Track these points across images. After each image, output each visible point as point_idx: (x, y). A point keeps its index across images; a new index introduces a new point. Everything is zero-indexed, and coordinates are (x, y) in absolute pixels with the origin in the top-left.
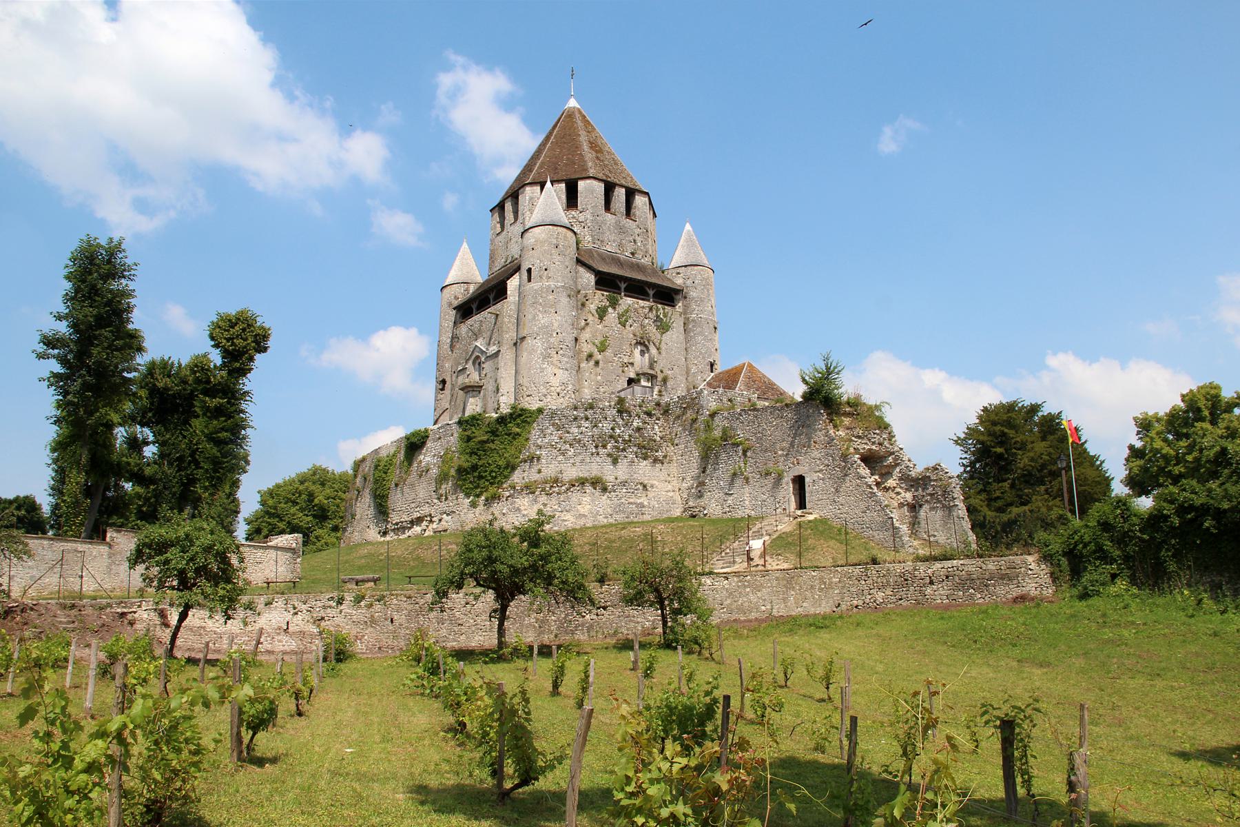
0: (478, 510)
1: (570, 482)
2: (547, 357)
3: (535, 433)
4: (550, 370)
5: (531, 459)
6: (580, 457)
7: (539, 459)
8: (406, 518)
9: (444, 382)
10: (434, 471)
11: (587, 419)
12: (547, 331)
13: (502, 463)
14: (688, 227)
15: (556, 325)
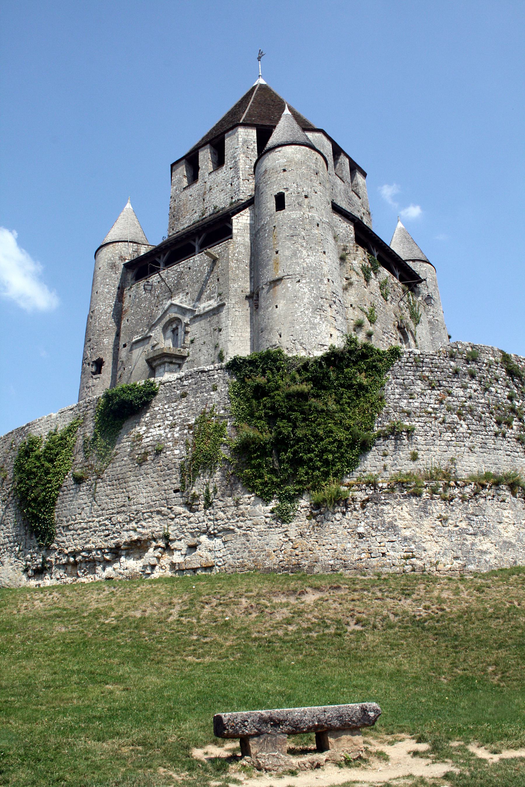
1: (472, 478)
3: (392, 390)
5: (395, 433)
6: (479, 439)
7: (410, 432)
8: (97, 541)
9: (99, 364)
10: (177, 453)
11: (473, 376)
12: (314, 273)
13: (341, 435)
15: (326, 269)
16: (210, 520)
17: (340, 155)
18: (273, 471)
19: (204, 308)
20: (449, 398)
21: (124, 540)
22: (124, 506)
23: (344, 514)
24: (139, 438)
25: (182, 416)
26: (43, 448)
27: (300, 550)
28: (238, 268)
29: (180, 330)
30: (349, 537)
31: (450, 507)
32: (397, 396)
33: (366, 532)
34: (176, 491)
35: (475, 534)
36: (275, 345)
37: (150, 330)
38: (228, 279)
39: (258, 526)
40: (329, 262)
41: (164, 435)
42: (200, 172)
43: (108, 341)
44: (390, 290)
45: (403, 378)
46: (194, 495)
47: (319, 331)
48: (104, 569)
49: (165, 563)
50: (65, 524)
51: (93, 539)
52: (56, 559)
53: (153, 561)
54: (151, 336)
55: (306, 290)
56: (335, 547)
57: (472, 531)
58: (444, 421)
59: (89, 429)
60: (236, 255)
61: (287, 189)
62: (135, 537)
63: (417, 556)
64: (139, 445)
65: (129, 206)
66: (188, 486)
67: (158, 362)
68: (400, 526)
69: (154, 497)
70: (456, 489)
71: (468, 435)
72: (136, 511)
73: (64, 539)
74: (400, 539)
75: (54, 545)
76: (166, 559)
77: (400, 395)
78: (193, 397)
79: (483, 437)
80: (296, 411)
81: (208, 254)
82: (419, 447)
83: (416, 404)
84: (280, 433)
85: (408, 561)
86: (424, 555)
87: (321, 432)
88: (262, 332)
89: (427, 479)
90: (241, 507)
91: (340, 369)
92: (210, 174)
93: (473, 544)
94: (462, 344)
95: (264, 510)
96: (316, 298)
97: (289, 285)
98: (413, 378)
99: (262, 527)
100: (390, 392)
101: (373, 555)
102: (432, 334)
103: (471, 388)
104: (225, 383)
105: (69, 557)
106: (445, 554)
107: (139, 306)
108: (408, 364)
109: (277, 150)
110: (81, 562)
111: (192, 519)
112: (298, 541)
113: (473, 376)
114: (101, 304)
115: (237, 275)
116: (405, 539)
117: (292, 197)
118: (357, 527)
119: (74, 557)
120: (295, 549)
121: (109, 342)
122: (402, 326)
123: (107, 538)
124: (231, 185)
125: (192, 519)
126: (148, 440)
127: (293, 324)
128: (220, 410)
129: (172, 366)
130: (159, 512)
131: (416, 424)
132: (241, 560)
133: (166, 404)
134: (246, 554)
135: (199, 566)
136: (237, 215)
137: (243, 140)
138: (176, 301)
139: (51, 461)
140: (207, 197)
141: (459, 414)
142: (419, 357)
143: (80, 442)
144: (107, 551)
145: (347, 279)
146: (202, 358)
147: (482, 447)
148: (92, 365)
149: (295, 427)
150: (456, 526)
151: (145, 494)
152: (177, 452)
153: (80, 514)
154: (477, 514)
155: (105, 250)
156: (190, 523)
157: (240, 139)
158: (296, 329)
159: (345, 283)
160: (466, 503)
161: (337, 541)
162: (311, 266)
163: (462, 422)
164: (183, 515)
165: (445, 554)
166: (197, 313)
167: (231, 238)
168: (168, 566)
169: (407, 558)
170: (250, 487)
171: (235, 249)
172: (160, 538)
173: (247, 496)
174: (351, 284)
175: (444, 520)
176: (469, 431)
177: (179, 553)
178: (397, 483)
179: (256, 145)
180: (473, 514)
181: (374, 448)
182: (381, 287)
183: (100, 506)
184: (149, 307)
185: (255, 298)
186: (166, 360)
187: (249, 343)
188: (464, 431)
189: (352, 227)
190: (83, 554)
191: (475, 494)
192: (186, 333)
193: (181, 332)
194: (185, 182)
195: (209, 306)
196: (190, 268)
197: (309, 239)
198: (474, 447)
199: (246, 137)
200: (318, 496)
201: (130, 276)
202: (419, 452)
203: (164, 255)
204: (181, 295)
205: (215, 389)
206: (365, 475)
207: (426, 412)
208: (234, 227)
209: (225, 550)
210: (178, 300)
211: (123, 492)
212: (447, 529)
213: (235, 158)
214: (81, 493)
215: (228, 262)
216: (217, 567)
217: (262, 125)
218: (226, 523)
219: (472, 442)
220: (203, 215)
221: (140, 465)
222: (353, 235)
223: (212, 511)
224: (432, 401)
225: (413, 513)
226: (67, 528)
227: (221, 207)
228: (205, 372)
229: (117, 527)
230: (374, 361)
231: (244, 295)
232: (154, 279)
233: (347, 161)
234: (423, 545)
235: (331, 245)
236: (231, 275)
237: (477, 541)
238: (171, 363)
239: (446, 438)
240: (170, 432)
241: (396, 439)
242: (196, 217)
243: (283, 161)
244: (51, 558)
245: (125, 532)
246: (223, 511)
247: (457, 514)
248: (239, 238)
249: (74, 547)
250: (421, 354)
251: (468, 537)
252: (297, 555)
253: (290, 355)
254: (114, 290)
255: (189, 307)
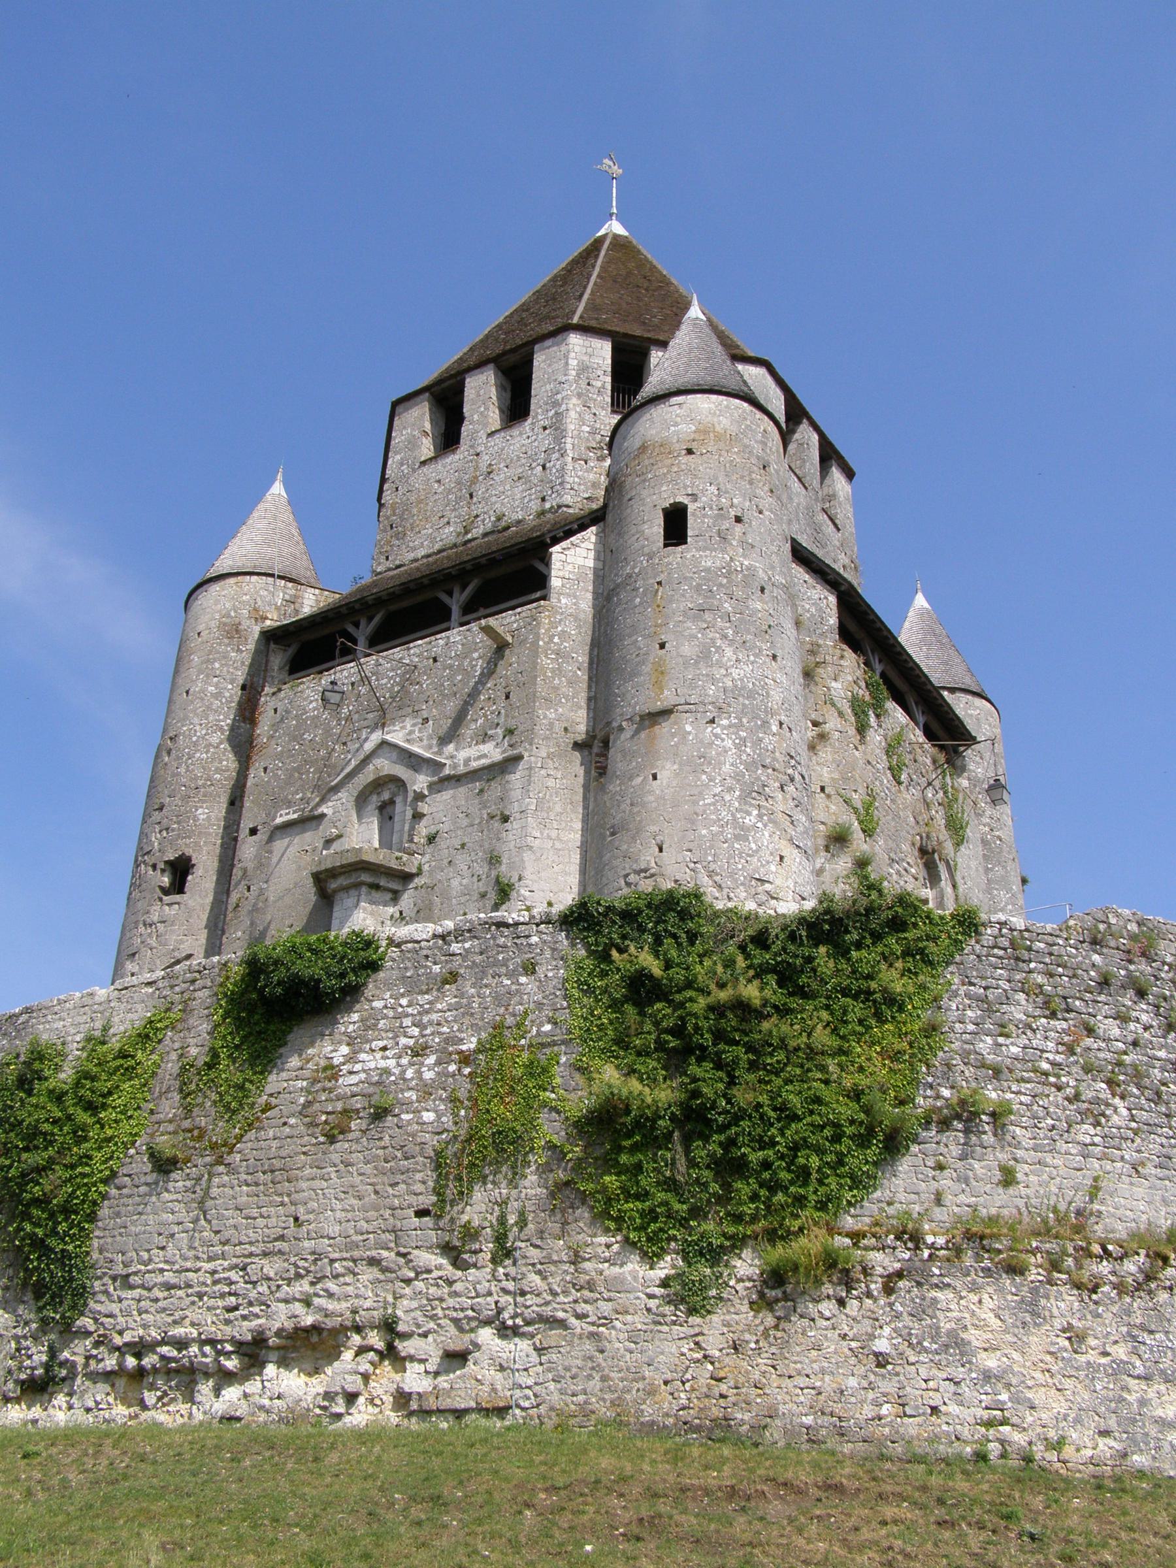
0: (714, 1331)
1: (1140, 1239)
2: (754, 793)
3: (959, 1011)
4: (767, 838)
5: (964, 1115)
6: (1154, 1145)
8: (203, 1320)
10: (429, 1120)
11: (1141, 994)
13: (845, 1110)
14: (920, 601)
15: (776, 696)
16: (505, 1291)
17: (799, 423)
18: (671, 1185)
19: (467, 761)
20: (1089, 1041)
21: (278, 1325)
22: (282, 1238)
23: (841, 1303)
24: (332, 1072)
25: (445, 1029)
26: (67, 1074)
27: (732, 1384)
28: (559, 672)
29: (399, 807)
30: (853, 1361)
31: (1092, 1307)
32: (971, 1027)
33: (894, 1352)
34: (421, 1213)
35: (1147, 1378)
36: (645, 871)
37: (323, 800)
38: (533, 697)
39: (629, 1318)
40: (781, 684)
41: (397, 1071)
42: (466, 429)
43: (209, 815)
44: (907, 759)
45: (984, 983)
46: (466, 1226)
47: (753, 846)
48: (217, 1392)
49: (380, 1391)
50: (119, 1270)
51: (193, 1315)
52: (88, 1358)
53: (353, 1383)
54: (323, 815)
55: (728, 743)
56: (818, 1384)
57: (1140, 1370)
58: (1077, 1097)
59: (198, 1036)
60: (556, 640)
61: (694, 497)
62: (309, 1320)
63: (1015, 1420)
64: (331, 1090)
65: (278, 488)
66: (453, 1203)
67: (342, 881)
68: (975, 1343)
69: (363, 1223)
70: (1105, 1263)
71: (1130, 1134)
72: (313, 1253)
73: (115, 1308)
74: (974, 1375)
75: (86, 1322)
76: (386, 1380)
77: (977, 1024)
78: (474, 985)
79: (1164, 1141)
80: (737, 1043)
81: (487, 630)
82: (1020, 1153)
83: (1014, 1050)
84: (696, 1094)
85: (991, 1431)
86: (1029, 1419)
87: (795, 1101)
88: (613, 834)
89: (1036, 1234)
90: (587, 1265)
91: (841, 951)
92: (491, 434)
93: (1143, 1402)
94: (1118, 916)
95: (642, 1276)
96: (751, 766)
97: (688, 728)
98: (1006, 986)
99: (638, 1320)
100: (953, 1015)
101: (909, 1411)
102: (987, 870)
103: (1137, 1020)
104: (558, 959)
105: (123, 1354)
106: (1078, 1421)
107: (297, 738)
108: (996, 951)
109: (675, 400)
110: (155, 1370)
111: (458, 1287)
112: (727, 1360)
113: (1141, 994)
114: (196, 720)
115: (556, 689)
116: (987, 1376)
117: (705, 516)
118: (872, 1337)
119: (138, 1356)
120: (719, 1380)
121: (209, 818)
122: (930, 848)
123: (231, 1315)
124: (544, 467)
125: (458, 1287)
126: (354, 1079)
127: (693, 822)
128: (541, 1024)
129: (376, 895)
130: (373, 1262)
131: (1016, 1095)
132: (581, 1398)
133: (403, 995)
134: (595, 1384)
135: (473, 1405)
136: (564, 544)
137: (577, 367)
138: (396, 736)
139: (91, 1107)
140: (480, 491)
141: (1110, 1083)
142: (1023, 938)
143: (172, 1066)
144: (229, 1348)
145: (815, 724)
146: (455, 883)
147: (1160, 1166)
148: (163, 871)
149: (732, 1082)
150: (1105, 1354)
151: (339, 1214)
152: (428, 1116)
153: (163, 1248)
154: (1153, 1327)
155: (215, 588)
156: (456, 1294)
157: (573, 363)
158: (702, 837)
159: (811, 733)
160: (1128, 1299)
161: (822, 1372)
162: (743, 688)
163: (1117, 1101)
164: (436, 1274)
165: (1078, 1421)
166: (447, 771)
167: (544, 598)
168: (388, 1399)
169: (989, 1424)
170: (611, 1218)
171: (554, 625)
172: (372, 1328)
173: (603, 1240)
174: (822, 736)
175: (1077, 1338)
176: (1134, 1125)
177: (421, 1368)
178: (969, 1236)
179: (609, 379)
180: (1142, 1328)
181: (914, 1148)
182: (890, 750)
183: (217, 1232)
184: (323, 744)
185: (595, 750)
186: (365, 877)
187: (576, 858)
188: (1122, 1124)
189: (832, 599)
190: (165, 1350)
191: (1149, 1278)
192: (418, 816)
193: (403, 811)
194: (427, 448)
195: (479, 758)
196: (435, 660)
197: (741, 621)
198: (1143, 1164)
199: (586, 358)
200: (779, 1252)
201: (278, 660)
202: (1019, 1167)
203: (370, 619)
204: (408, 723)
205: (530, 969)
206: (891, 1210)
207: (1035, 1071)
208: (553, 573)
209: (540, 1369)
210: (401, 734)
211: (282, 1204)
212: (1082, 1359)
213: (556, 404)
214: (166, 1196)
215: (536, 655)
216: (517, 1411)
217: (626, 335)
218: (547, 1303)
219: (1139, 1151)
220: (466, 533)
221: (332, 1139)
222: (833, 621)
223: (512, 1271)
224: (1051, 1045)
225: (1006, 1315)
226: (125, 1281)
227: (515, 517)
228: (507, 925)
229: (260, 1289)
230: (920, 939)
231: (570, 739)
232: (345, 673)
233: (815, 437)
234: (1030, 1395)
235: (788, 640)
236: (541, 688)
237: (1151, 1394)
238: (376, 887)
239: (1080, 1138)
240: (411, 1064)
241: (967, 1131)
242: (449, 534)
243: (687, 429)
244: (75, 1353)
245: (282, 1305)
246: (539, 1273)
247: (1107, 1324)
248: (564, 601)
249: (141, 1332)
250: (1027, 930)
251: (1132, 1383)
252: (722, 1396)
253: (719, 906)
254: (232, 692)
255: (428, 755)
